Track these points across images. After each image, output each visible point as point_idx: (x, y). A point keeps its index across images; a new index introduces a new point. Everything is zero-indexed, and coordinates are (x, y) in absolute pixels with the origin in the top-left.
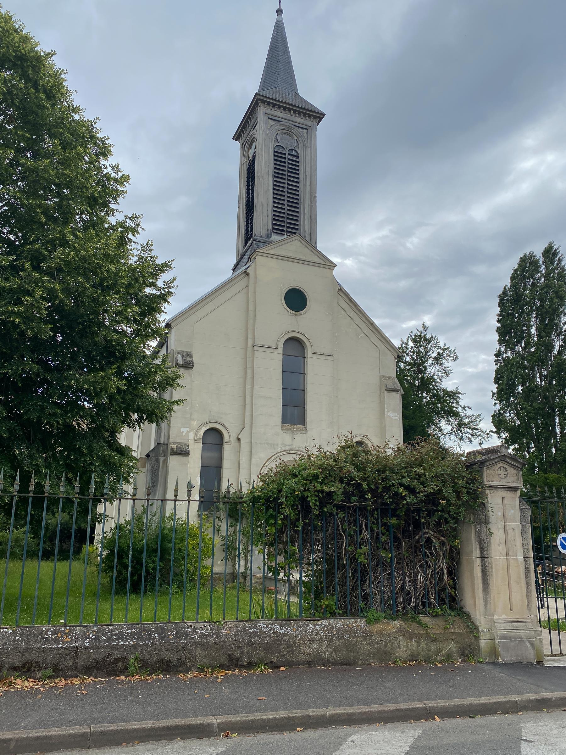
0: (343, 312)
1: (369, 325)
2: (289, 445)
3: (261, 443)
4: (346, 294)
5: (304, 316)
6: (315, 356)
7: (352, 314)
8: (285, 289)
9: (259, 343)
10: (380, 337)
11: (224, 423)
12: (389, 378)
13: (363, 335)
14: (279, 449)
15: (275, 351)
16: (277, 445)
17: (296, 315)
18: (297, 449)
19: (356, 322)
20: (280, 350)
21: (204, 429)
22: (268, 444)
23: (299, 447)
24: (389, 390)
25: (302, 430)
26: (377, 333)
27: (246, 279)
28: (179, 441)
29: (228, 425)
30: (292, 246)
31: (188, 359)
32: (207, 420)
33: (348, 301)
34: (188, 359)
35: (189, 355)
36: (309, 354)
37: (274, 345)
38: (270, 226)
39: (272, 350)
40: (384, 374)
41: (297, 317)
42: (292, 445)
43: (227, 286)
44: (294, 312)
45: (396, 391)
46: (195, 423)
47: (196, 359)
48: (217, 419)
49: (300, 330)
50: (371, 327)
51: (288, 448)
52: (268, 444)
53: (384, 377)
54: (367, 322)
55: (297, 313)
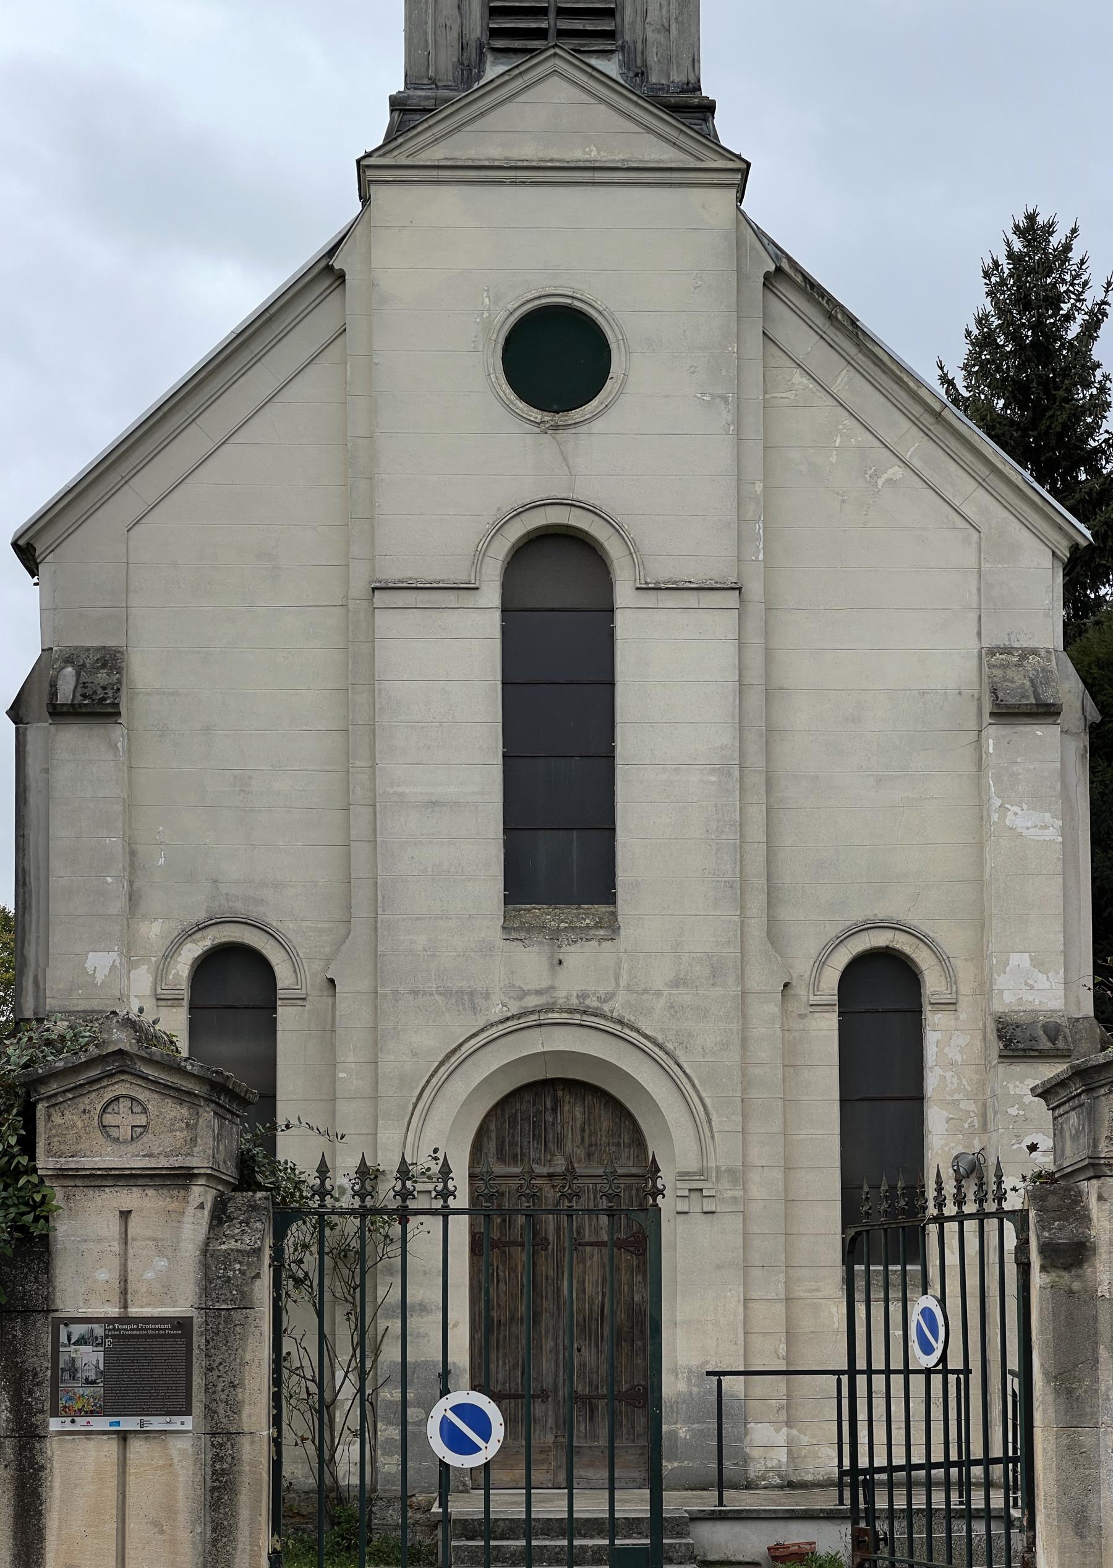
0: (799, 378)
1: (928, 419)
2: (539, 992)
3: (414, 993)
4: (812, 289)
5: (598, 426)
6: (650, 599)
7: (845, 381)
8: (503, 314)
9: (392, 573)
10: (983, 470)
11: (272, 920)
12: (1025, 654)
13: (896, 471)
14: (496, 1012)
15: (467, 599)
16: (487, 995)
17: (556, 427)
18: (574, 1001)
19: (864, 417)
20: (491, 595)
21: (193, 951)
22: (446, 993)
23: (583, 996)
24: (1006, 712)
25: (597, 926)
26: (968, 457)
27: (334, 299)
28: (82, 1005)
29: (288, 928)
30: (554, 108)
31: (102, 677)
32: (200, 916)
33: (820, 321)
34: (102, 677)
35: (111, 660)
36: (624, 594)
37: (459, 574)
38: (476, 28)
39: (450, 598)
40: (1002, 641)
41: (562, 435)
42: (552, 988)
43: (256, 347)
44: (547, 417)
45: (1047, 712)
46: (154, 932)
47: (144, 672)
48: (241, 908)
49: (583, 493)
50: (937, 430)
51: (532, 1002)
52: (446, 993)
53: (992, 652)
54: (917, 410)
55: (560, 418)
